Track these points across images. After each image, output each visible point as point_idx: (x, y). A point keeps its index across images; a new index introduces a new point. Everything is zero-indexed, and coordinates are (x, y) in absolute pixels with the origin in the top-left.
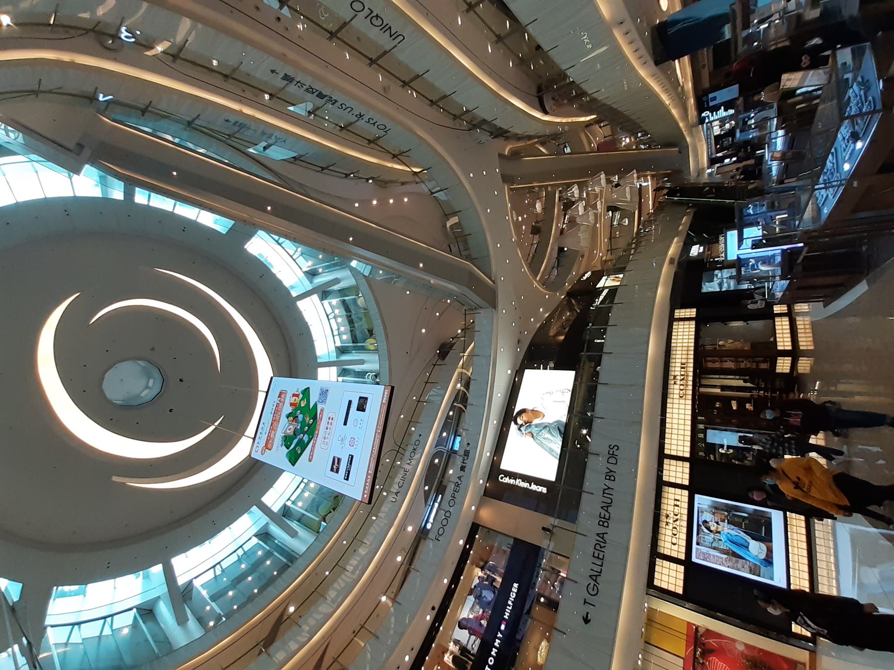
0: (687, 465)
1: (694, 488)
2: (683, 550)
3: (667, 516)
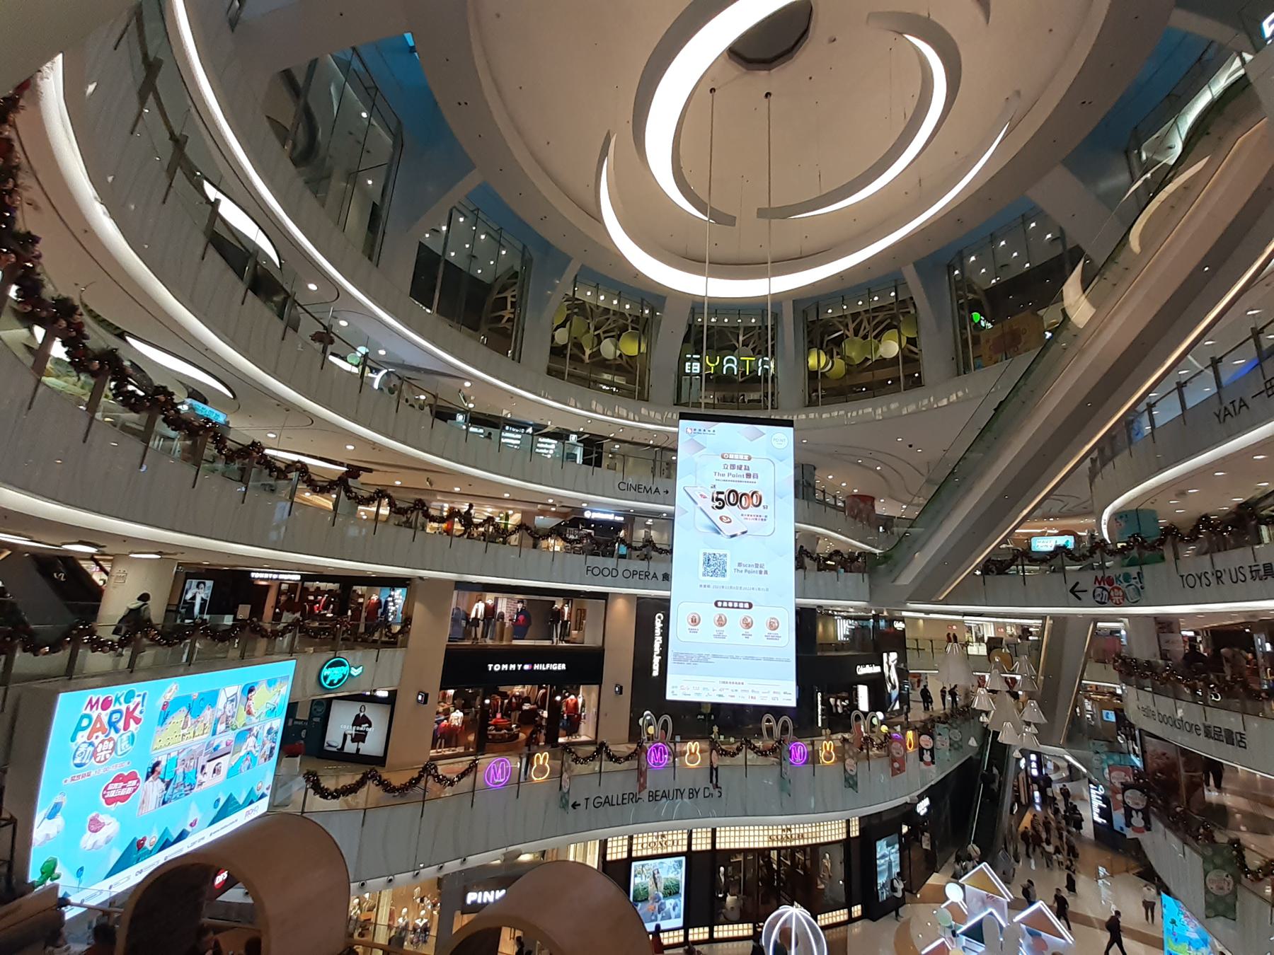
0: (709, 847)
1: (690, 855)
2: (639, 854)
3: (663, 836)
